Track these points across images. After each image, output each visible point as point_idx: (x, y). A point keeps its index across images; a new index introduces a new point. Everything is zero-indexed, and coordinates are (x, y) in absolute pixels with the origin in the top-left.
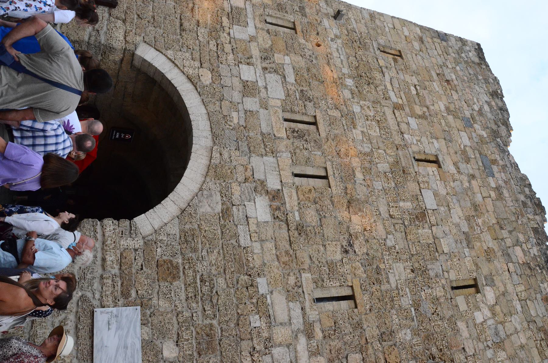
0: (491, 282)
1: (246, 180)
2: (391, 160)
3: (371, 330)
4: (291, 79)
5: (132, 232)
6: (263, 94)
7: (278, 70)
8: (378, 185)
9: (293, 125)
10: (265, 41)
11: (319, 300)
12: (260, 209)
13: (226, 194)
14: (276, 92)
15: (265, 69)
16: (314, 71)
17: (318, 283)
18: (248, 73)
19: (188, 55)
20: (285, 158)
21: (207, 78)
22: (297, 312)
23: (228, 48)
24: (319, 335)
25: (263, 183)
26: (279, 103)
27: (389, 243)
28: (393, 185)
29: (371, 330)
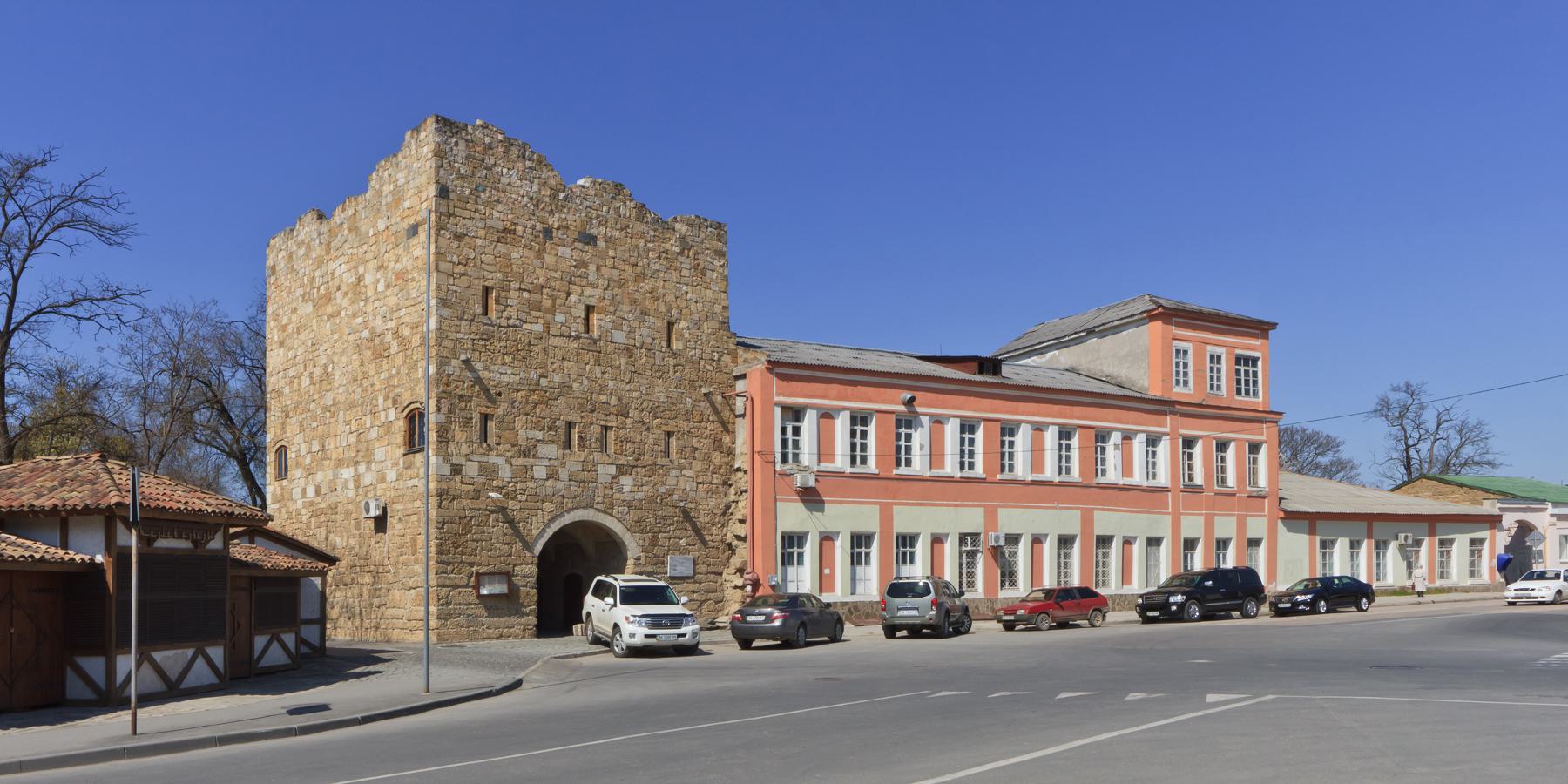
3: (685, 426)
4: (539, 435)
8: (611, 383)
12: (627, 482)
14: (550, 451)
18: (540, 472)
29: (685, 426)
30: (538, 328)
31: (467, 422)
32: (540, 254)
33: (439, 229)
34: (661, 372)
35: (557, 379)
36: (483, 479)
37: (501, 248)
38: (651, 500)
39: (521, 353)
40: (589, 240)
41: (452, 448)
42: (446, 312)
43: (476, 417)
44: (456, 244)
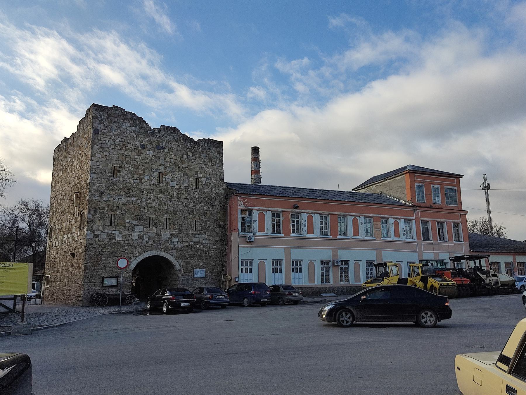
0: (196, 173)
3: (202, 217)
4: (136, 222)
5: (180, 270)
8: (169, 202)
12: (176, 240)
13: (172, 248)
14: (141, 228)
15: (132, 230)
18: (135, 237)
21: (138, 250)
23: (126, 242)
29: (202, 217)
30: (137, 181)
31: (102, 218)
33: (93, 144)
37: (121, 152)
38: (187, 247)
39: (129, 191)
40: (163, 148)
42: (95, 176)
43: (106, 215)
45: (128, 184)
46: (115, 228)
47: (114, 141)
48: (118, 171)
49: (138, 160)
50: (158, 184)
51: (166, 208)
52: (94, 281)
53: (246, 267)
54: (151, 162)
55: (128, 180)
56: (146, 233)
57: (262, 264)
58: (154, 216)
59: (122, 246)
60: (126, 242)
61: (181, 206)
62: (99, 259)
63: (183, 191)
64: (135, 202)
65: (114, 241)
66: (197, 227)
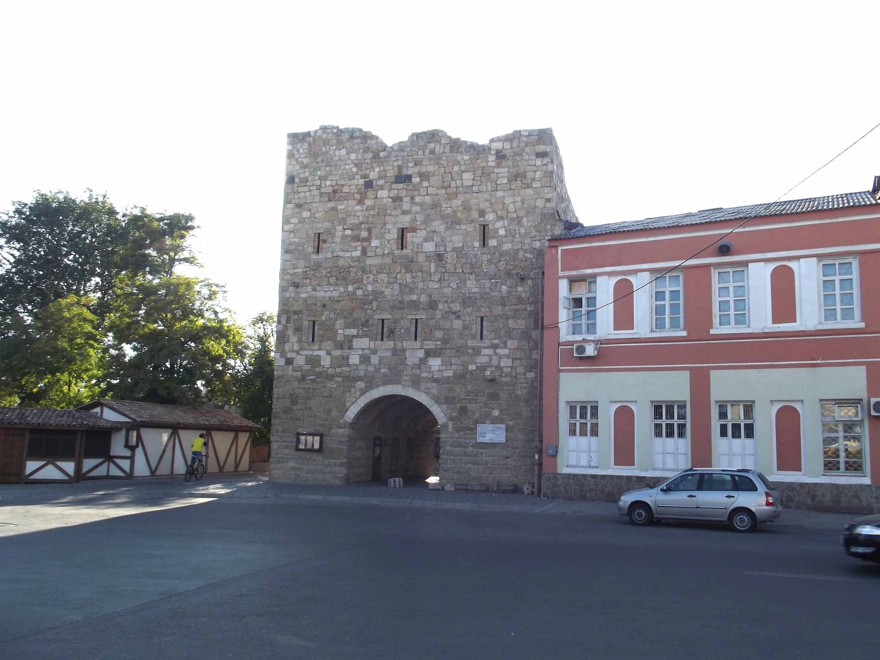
0: (482, 213)
1: (420, 368)
2: (403, 271)
3: (498, 310)
4: (354, 332)
5: (445, 426)
6: (367, 352)
7: (350, 339)
8: (421, 285)
9: (385, 335)
10: (328, 345)
11: (481, 338)
12: (435, 363)
14: (363, 343)
15: (350, 348)
16: (346, 313)
17: (473, 337)
18: (354, 359)
19: (347, 394)
20: (406, 344)
21: (361, 385)
22: (486, 351)
23: (338, 370)
24: (496, 341)
25: (421, 360)
26: (372, 343)
27: (455, 287)
28: (420, 273)
29: (498, 310)
30: (357, 253)
31: (298, 329)
32: (360, 202)
34: (474, 269)
35: (370, 288)
36: (308, 367)
37: (331, 205)
38: (460, 377)
40: (409, 178)
41: (287, 347)
42: (288, 257)
43: (306, 323)
44: (297, 210)
45: (341, 262)
46: (320, 346)
47: (319, 187)
48: (325, 241)
49: (359, 214)
50: (397, 252)
51: (414, 297)
52: (286, 439)
53: (583, 421)
54: (382, 213)
55: (340, 254)
56: (374, 352)
57: (624, 416)
58: (390, 317)
59: (331, 378)
60: (338, 370)
61: (446, 290)
62: (294, 402)
63: (450, 258)
64: (354, 293)
65: (317, 369)
66: (485, 332)
